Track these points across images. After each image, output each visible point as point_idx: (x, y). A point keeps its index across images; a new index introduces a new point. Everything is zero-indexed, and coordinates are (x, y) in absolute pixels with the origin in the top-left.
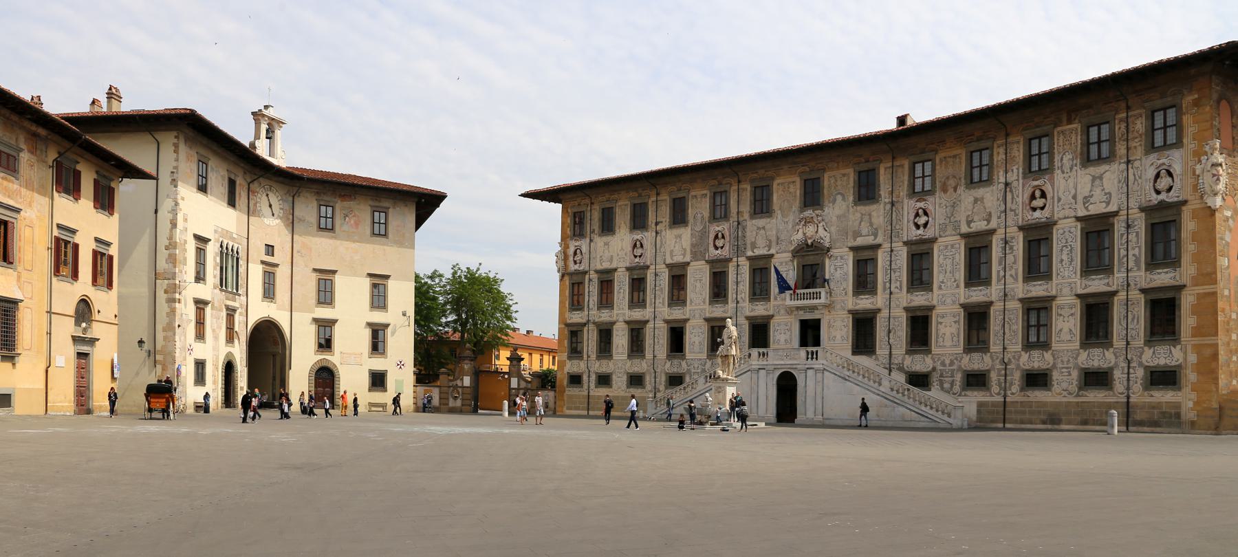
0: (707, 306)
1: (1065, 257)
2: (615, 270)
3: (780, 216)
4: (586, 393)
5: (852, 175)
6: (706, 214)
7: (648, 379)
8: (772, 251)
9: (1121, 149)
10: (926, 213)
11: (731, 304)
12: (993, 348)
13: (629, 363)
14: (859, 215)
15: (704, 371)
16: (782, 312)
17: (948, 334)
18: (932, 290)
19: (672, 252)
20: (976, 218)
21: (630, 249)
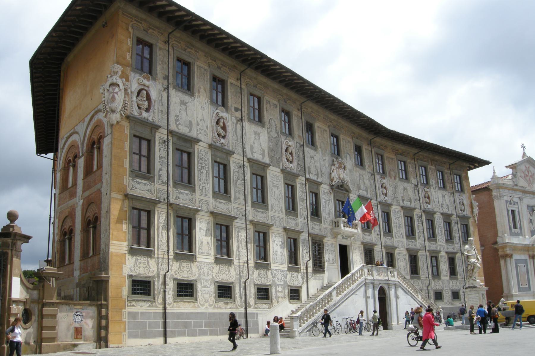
0: (283, 215)
1: (440, 232)
2: (197, 141)
3: (320, 153)
4: (160, 309)
5: (352, 144)
6: (279, 125)
7: (237, 291)
8: (319, 180)
9: (448, 186)
10: (385, 188)
11: (300, 220)
12: (422, 277)
13: (216, 268)
14: (357, 174)
15: (286, 282)
16: (329, 235)
17: (402, 267)
18: (392, 237)
19: (252, 147)
20: (406, 199)
21: (214, 124)
